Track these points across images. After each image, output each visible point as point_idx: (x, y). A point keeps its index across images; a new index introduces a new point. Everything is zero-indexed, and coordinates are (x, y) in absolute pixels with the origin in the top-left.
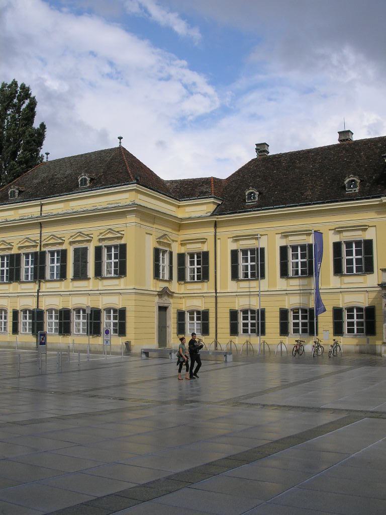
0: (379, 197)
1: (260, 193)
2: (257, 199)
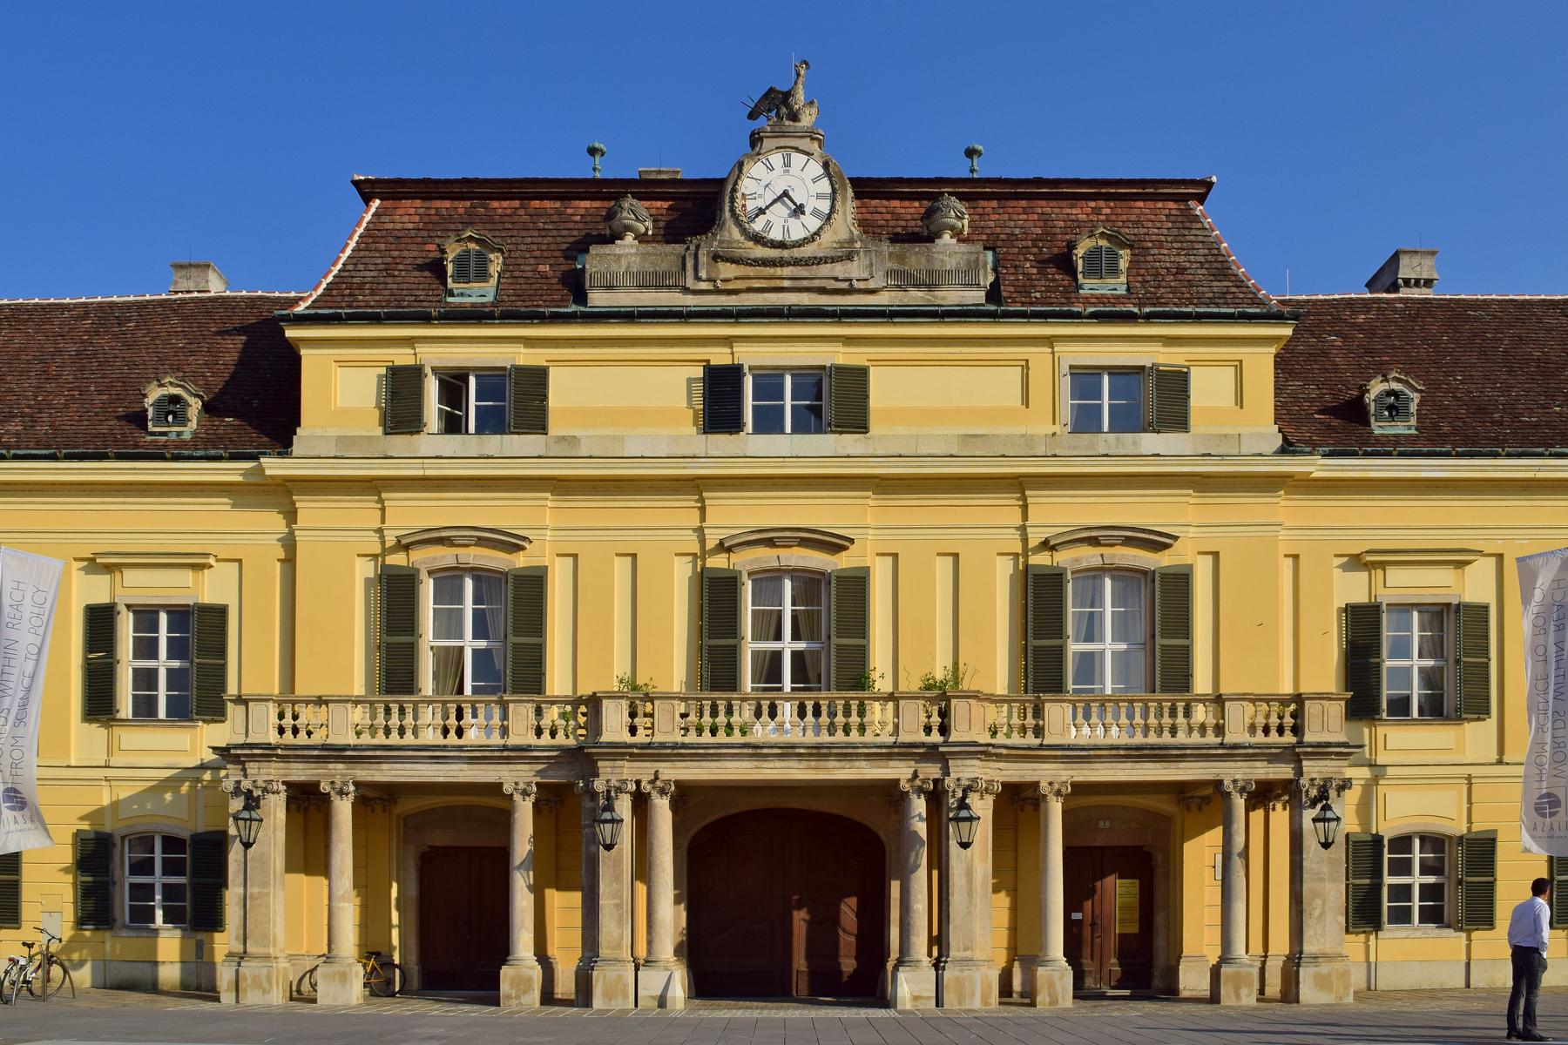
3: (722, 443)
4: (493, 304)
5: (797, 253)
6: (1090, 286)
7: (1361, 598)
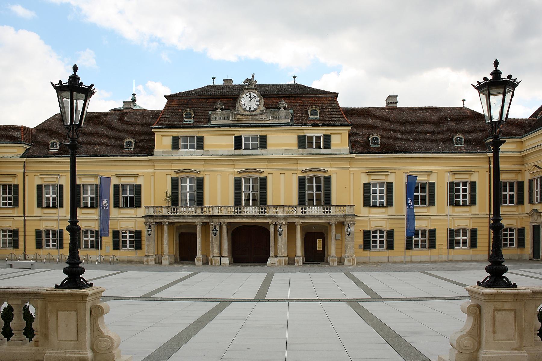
0: (147, 156)
1: (61, 144)
2: (58, 148)
3: (238, 152)
4: (192, 124)
5: (252, 113)
6: (312, 118)
7: (367, 181)
